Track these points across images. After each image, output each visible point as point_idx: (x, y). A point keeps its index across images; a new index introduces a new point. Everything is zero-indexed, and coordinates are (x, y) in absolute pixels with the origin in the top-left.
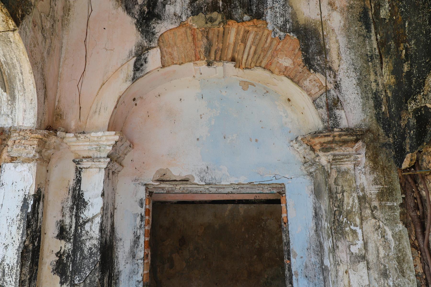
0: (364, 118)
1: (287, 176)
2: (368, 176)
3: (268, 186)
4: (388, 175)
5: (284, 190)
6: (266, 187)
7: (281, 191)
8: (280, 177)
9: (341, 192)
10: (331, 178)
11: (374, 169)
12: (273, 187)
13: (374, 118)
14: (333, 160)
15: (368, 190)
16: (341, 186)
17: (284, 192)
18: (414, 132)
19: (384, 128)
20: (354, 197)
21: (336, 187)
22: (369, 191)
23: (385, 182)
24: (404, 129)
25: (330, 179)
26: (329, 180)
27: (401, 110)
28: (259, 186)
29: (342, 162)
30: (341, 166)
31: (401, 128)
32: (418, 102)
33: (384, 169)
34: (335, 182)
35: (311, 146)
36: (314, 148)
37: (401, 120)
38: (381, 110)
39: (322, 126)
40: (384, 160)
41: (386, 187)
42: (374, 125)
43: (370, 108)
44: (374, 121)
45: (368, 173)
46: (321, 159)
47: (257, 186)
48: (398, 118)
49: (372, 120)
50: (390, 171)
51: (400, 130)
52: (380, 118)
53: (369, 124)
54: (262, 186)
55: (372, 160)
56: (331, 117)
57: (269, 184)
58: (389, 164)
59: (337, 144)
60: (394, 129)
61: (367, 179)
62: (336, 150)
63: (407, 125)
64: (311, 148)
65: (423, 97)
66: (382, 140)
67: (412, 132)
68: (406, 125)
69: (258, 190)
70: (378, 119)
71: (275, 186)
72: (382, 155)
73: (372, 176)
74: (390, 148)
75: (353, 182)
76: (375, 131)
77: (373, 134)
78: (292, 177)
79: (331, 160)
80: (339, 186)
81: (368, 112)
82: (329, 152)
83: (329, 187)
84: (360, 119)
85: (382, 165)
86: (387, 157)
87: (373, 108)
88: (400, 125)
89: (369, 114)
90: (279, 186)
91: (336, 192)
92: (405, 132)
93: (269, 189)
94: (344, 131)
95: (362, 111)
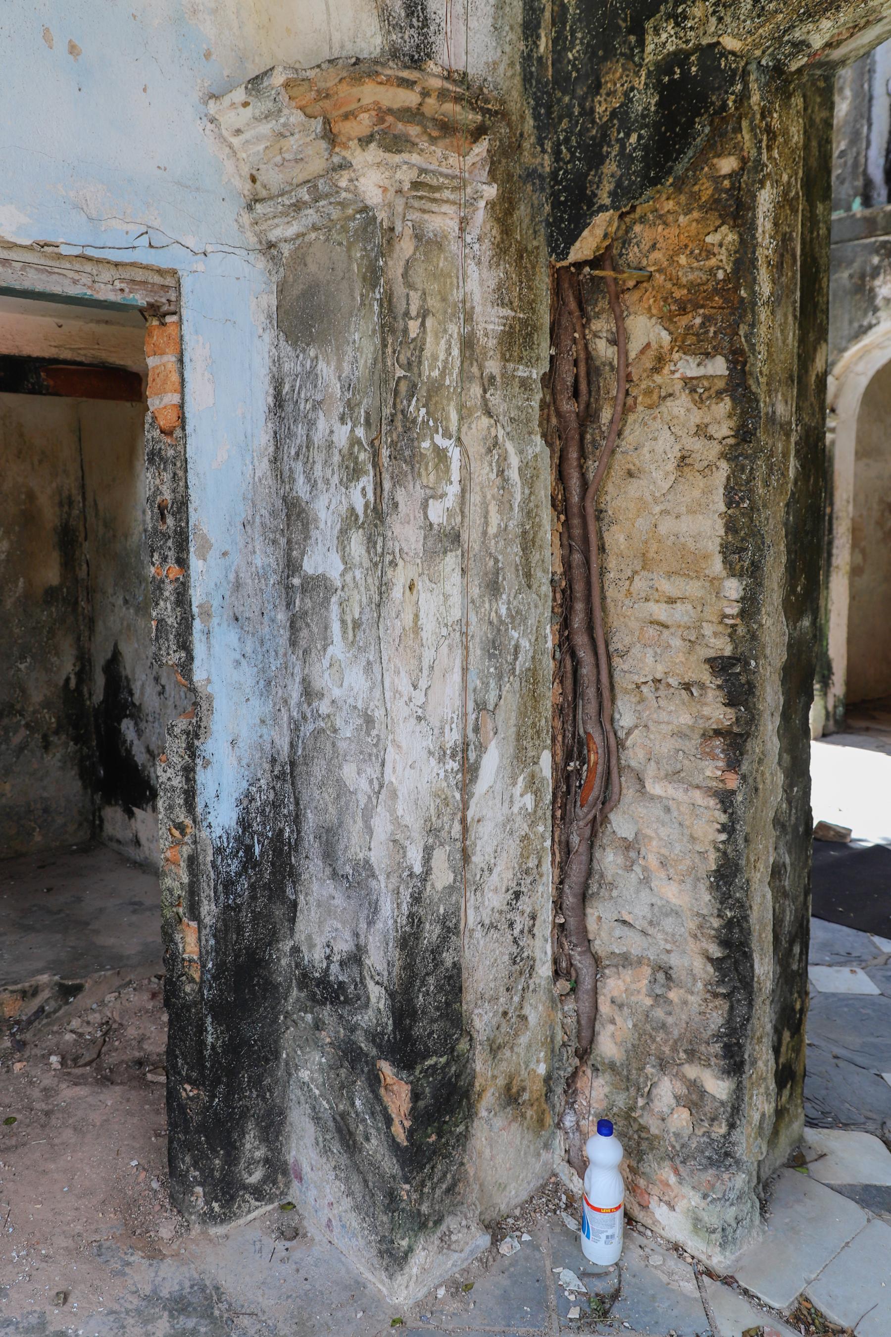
0: (495, 58)
1: (190, 242)
2: (485, 274)
3: (113, 271)
4: (529, 280)
5: (173, 299)
6: (106, 275)
7: (164, 300)
8: (164, 241)
9: (418, 316)
10: (395, 256)
11: (501, 250)
12: (133, 281)
13: (518, 67)
14: (416, 185)
15: (480, 319)
16: (420, 293)
17: (172, 308)
18: (640, 137)
19: (536, 117)
20: (451, 336)
21: (408, 295)
22: (484, 325)
23: (520, 299)
24: (605, 129)
25: (392, 258)
26: (390, 263)
27: (605, 59)
28: (77, 267)
29: (434, 200)
30: (426, 216)
31: (593, 122)
32: (692, 28)
33: (522, 257)
34: (405, 275)
35: (327, 122)
36: (335, 130)
37: (598, 93)
38: (538, 47)
39: (378, 40)
40: (524, 226)
41: (521, 316)
42: (515, 94)
43: (512, 28)
44: (517, 80)
45: (485, 259)
46: (362, 180)
47: (68, 266)
48: (589, 87)
49: (513, 75)
50: (534, 267)
51: (588, 130)
52: (531, 73)
53: (505, 88)
54: (88, 267)
55: (498, 220)
56: (413, 13)
57: (116, 265)
58: (535, 243)
59: (425, 127)
60: (564, 124)
61: (482, 282)
62: (422, 150)
63: (620, 115)
64: (325, 128)
65: (714, 12)
66: (526, 158)
67: (633, 138)
68: (614, 114)
69: (75, 282)
70: (527, 78)
71: (139, 275)
72: (522, 208)
73: (494, 273)
74: (542, 189)
75: (451, 283)
76: (514, 118)
77: (509, 125)
78: (209, 249)
79: (406, 186)
80: (416, 290)
81: (508, 39)
82: (400, 152)
83: (385, 291)
84: (484, 59)
85: (520, 243)
86: (533, 218)
87: (519, 30)
88: (592, 110)
89: (508, 48)
90: (157, 279)
91: (407, 314)
92: (604, 137)
93: (118, 285)
94: (454, 81)
95: (492, 29)
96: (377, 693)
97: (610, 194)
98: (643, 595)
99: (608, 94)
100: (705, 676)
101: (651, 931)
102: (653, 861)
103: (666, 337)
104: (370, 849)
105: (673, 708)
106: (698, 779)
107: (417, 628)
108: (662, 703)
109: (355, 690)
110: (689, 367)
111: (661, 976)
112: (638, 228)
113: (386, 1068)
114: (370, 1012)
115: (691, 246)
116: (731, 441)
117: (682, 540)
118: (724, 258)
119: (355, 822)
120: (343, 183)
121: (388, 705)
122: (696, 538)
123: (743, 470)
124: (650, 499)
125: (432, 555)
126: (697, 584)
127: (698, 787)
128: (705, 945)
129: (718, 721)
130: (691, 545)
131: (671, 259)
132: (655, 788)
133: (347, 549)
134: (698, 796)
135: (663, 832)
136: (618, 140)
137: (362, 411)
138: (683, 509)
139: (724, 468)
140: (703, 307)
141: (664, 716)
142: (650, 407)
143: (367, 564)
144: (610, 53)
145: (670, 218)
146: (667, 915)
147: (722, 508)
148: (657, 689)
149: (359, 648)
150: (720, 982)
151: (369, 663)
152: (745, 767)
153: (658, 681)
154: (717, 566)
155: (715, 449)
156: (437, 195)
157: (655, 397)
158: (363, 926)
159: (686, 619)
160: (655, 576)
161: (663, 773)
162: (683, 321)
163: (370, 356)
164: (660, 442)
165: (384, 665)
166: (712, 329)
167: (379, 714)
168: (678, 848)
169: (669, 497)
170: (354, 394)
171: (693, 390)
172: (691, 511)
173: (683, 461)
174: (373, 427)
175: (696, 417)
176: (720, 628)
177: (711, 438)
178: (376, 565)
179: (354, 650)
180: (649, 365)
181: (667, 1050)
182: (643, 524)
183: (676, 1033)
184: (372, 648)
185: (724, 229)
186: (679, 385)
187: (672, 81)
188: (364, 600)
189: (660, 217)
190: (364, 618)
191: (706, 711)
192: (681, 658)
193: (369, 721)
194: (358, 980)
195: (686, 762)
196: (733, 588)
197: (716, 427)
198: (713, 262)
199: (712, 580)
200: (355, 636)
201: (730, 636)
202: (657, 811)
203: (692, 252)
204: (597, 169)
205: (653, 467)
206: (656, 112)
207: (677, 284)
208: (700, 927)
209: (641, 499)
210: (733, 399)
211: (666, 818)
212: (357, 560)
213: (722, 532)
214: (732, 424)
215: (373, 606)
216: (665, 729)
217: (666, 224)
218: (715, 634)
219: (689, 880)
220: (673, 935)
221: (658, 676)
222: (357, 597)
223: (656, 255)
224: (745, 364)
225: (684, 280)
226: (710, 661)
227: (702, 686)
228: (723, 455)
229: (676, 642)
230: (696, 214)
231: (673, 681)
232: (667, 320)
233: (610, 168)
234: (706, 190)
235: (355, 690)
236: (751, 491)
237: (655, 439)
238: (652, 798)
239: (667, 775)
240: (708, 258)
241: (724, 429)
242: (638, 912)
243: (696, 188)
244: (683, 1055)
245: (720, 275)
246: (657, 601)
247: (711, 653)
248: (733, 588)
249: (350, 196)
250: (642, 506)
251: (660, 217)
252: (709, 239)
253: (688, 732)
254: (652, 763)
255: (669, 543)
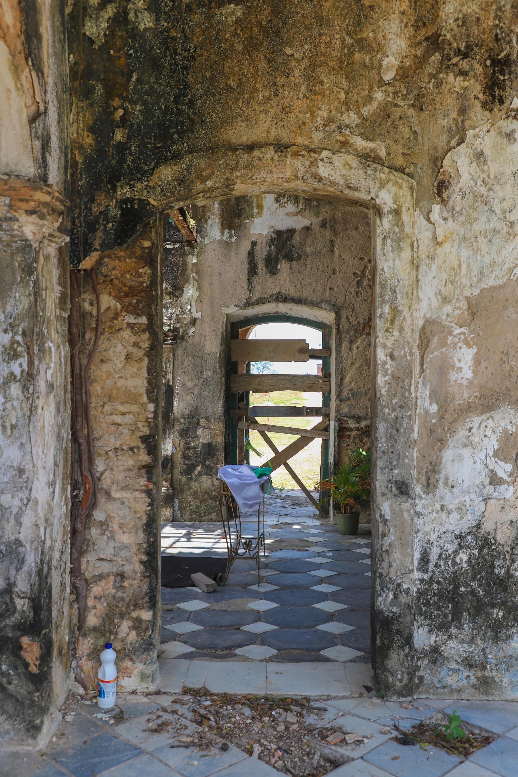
18: (113, 225)
24: (97, 218)
31: (91, 213)
37: (93, 203)
48: (89, 199)
51: (89, 216)
63: (104, 214)
67: (110, 225)
68: (101, 213)
88: (91, 209)
92: (97, 222)
96: (28, 457)
97: (100, 245)
98: (109, 412)
99: (98, 204)
100: (140, 444)
101: (115, 559)
102: (116, 527)
103: (119, 306)
104: (19, 533)
105: (125, 459)
106: (137, 487)
107: (44, 427)
108: (119, 457)
109: (12, 458)
110: (131, 319)
111: (119, 578)
112: (106, 260)
113: (25, 640)
114: (16, 615)
115: (131, 272)
116: (148, 349)
117: (129, 389)
118: (146, 279)
119: (8, 522)
120: (16, 227)
121: (35, 462)
122: (135, 387)
123: (153, 361)
124: (113, 372)
125: (48, 393)
126: (136, 406)
127: (137, 490)
128: (140, 557)
129: (146, 461)
130: (133, 390)
131: (122, 275)
132: (116, 495)
133: (8, 392)
134: (137, 494)
135: (121, 513)
136: (103, 224)
137: (21, 329)
138: (129, 376)
139: (146, 361)
140: (136, 296)
141: (120, 463)
142: (111, 333)
143: (21, 397)
144: (99, 188)
145: (122, 259)
146: (122, 550)
147: (146, 375)
148: (116, 452)
149: (15, 438)
150: (146, 571)
151: (22, 444)
152: (154, 479)
153: (116, 449)
154: (145, 399)
155: (141, 353)
156: (53, 239)
157: (114, 329)
158: (13, 572)
159: (130, 421)
160: (115, 404)
161: (119, 488)
162: (127, 300)
163: (27, 305)
164: (118, 348)
165: (33, 444)
166: (141, 305)
167: (28, 467)
168: (128, 518)
169: (122, 371)
170: (14, 321)
171: (132, 328)
172: (132, 377)
173: (128, 357)
174: (28, 336)
175: (133, 339)
176: (145, 424)
177: (140, 347)
178: (28, 398)
179: (12, 439)
180: (111, 316)
181: (124, 609)
182: (109, 382)
183: (128, 600)
184: (25, 437)
185: (146, 268)
186: (125, 326)
187: (127, 207)
188: (20, 415)
189: (117, 257)
190: (19, 423)
191: (140, 458)
192: (128, 437)
193: (21, 471)
194: (8, 601)
195: (131, 481)
196: (151, 407)
197: (143, 343)
198: (141, 279)
199: (142, 405)
200: (12, 432)
201: (149, 426)
202: (117, 504)
203: (132, 274)
204: (93, 233)
205: (115, 358)
206: (120, 217)
207: (125, 285)
208: (139, 549)
209: (109, 371)
210: (149, 333)
211: (122, 507)
212: (15, 396)
213: (146, 385)
214: (149, 343)
215: (26, 417)
216: (121, 468)
217: (120, 260)
218: (143, 426)
219: (133, 531)
220: (126, 557)
221: (117, 446)
222: (15, 414)
223: (114, 272)
224: (152, 320)
225: (128, 284)
226: (141, 437)
227: (138, 448)
228: (145, 355)
229: (126, 431)
230: (134, 260)
231: (125, 447)
232: (118, 298)
233: (99, 234)
234: (139, 252)
235: (12, 458)
236: (156, 369)
237: (115, 347)
238: (115, 499)
239: (122, 489)
240: (139, 277)
241: (146, 345)
242: (108, 552)
243: (134, 250)
244: (132, 608)
245: (145, 285)
246: (116, 415)
247: (141, 434)
248: (151, 407)
249: (19, 234)
250: (109, 374)
251: (117, 257)
252: (140, 270)
253: (132, 468)
254: (115, 485)
255: (123, 390)
